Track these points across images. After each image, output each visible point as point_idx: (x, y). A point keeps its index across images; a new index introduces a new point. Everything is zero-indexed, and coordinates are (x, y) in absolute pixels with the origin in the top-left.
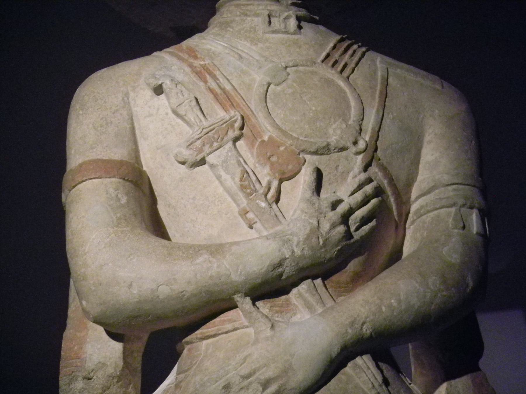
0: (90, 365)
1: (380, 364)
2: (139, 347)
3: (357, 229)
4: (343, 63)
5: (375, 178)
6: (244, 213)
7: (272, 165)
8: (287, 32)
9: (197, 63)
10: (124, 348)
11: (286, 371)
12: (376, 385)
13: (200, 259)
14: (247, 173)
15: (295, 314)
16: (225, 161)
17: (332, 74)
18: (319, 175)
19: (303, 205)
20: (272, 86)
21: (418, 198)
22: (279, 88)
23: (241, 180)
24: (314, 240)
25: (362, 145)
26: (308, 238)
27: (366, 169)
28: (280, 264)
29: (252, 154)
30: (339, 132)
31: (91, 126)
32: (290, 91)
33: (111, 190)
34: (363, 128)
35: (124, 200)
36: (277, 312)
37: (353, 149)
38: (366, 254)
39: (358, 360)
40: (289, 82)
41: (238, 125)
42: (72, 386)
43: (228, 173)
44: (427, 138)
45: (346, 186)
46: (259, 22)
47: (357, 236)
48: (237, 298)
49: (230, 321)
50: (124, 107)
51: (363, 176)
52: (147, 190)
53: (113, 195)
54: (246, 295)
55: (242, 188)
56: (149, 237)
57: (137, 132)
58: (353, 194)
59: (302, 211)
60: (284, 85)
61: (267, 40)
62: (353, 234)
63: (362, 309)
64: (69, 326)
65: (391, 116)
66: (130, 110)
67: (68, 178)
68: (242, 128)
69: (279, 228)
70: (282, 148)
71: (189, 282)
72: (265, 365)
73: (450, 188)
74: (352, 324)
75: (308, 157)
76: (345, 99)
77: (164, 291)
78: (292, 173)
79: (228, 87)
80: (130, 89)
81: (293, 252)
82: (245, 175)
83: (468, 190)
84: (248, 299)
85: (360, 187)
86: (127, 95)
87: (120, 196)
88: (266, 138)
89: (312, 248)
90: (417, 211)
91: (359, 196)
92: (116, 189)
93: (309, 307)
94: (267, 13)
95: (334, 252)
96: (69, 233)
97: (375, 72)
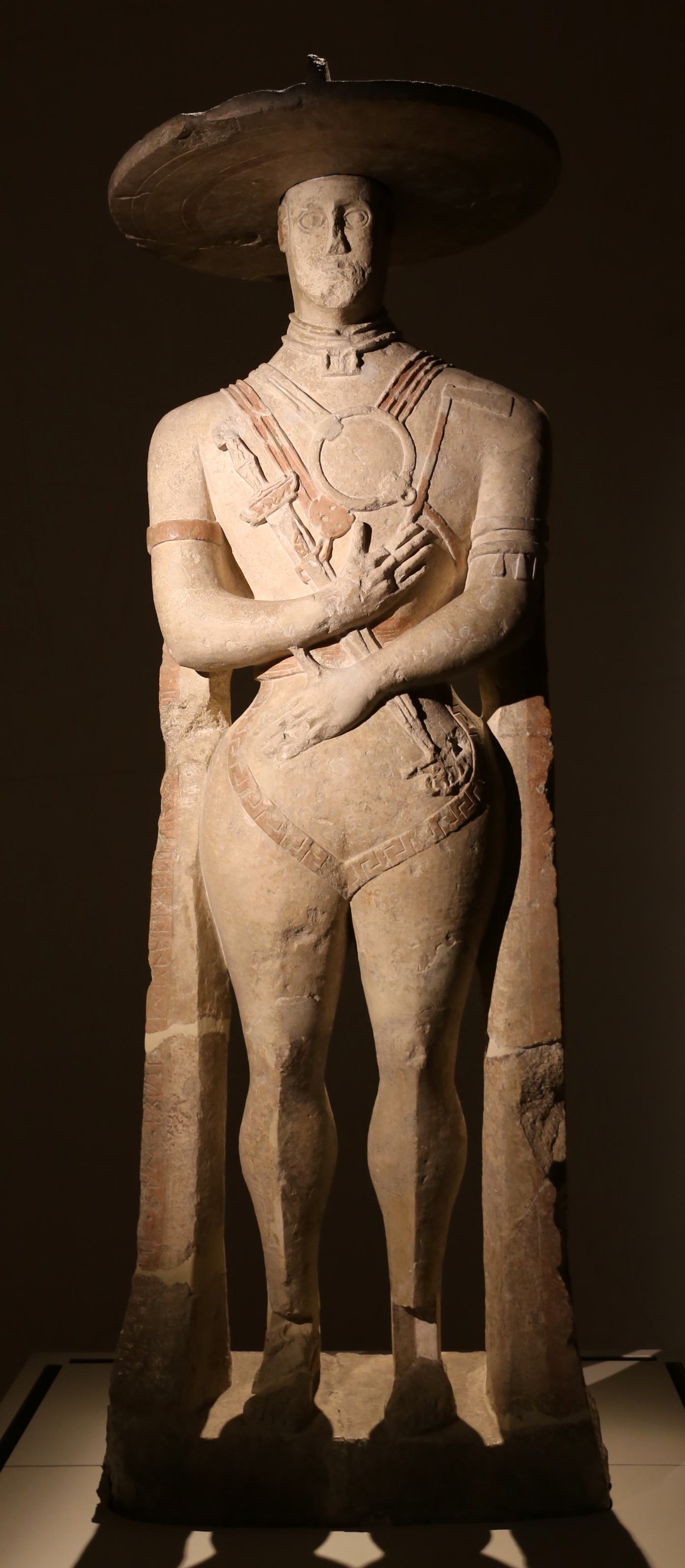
0: (183, 696)
1: (421, 700)
3: (403, 580)
4: (401, 404)
5: (426, 526)
6: (300, 571)
7: (324, 524)
8: (346, 374)
9: (259, 414)
10: (210, 683)
11: (327, 713)
12: (410, 720)
13: (259, 619)
14: (301, 534)
15: (344, 660)
16: (282, 522)
17: (387, 421)
18: (367, 530)
19: (349, 565)
20: (326, 442)
21: (476, 536)
22: (333, 444)
23: (295, 542)
24: (356, 599)
25: (411, 496)
26: (350, 597)
27: (415, 519)
29: (306, 514)
30: (388, 487)
31: (166, 483)
32: (343, 446)
33: (186, 552)
34: (414, 477)
35: (197, 560)
36: (328, 659)
37: (402, 502)
39: (397, 699)
40: (342, 436)
41: (293, 486)
42: (170, 713)
43: (285, 534)
44: (485, 477)
46: (321, 360)
47: (402, 586)
48: (292, 650)
49: (290, 666)
50: (194, 462)
51: (412, 527)
52: (220, 540)
53: (188, 556)
54: (299, 647)
55: (297, 548)
56: (219, 595)
57: (208, 485)
58: (399, 547)
59: (347, 571)
60: (337, 440)
61: (326, 384)
63: (396, 659)
64: (164, 661)
65: (445, 460)
66: (201, 464)
67: (150, 534)
68: (297, 489)
69: (329, 585)
70: (333, 508)
71: (250, 639)
72: (312, 707)
73: (499, 532)
74: (386, 672)
75: (356, 514)
76: (398, 449)
77: (231, 646)
78: (342, 532)
79: (286, 445)
80: (199, 441)
81: (336, 611)
82: (299, 537)
83: (514, 535)
84: (301, 650)
85: (408, 539)
86: (197, 449)
87: (194, 556)
88: (319, 498)
89: (354, 607)
90: (476, 549)
92: (190, 550)
93: (356, 654)
94: (325, 353)
95: (377, 605)
96: (154, 587)
97: (436, 408)
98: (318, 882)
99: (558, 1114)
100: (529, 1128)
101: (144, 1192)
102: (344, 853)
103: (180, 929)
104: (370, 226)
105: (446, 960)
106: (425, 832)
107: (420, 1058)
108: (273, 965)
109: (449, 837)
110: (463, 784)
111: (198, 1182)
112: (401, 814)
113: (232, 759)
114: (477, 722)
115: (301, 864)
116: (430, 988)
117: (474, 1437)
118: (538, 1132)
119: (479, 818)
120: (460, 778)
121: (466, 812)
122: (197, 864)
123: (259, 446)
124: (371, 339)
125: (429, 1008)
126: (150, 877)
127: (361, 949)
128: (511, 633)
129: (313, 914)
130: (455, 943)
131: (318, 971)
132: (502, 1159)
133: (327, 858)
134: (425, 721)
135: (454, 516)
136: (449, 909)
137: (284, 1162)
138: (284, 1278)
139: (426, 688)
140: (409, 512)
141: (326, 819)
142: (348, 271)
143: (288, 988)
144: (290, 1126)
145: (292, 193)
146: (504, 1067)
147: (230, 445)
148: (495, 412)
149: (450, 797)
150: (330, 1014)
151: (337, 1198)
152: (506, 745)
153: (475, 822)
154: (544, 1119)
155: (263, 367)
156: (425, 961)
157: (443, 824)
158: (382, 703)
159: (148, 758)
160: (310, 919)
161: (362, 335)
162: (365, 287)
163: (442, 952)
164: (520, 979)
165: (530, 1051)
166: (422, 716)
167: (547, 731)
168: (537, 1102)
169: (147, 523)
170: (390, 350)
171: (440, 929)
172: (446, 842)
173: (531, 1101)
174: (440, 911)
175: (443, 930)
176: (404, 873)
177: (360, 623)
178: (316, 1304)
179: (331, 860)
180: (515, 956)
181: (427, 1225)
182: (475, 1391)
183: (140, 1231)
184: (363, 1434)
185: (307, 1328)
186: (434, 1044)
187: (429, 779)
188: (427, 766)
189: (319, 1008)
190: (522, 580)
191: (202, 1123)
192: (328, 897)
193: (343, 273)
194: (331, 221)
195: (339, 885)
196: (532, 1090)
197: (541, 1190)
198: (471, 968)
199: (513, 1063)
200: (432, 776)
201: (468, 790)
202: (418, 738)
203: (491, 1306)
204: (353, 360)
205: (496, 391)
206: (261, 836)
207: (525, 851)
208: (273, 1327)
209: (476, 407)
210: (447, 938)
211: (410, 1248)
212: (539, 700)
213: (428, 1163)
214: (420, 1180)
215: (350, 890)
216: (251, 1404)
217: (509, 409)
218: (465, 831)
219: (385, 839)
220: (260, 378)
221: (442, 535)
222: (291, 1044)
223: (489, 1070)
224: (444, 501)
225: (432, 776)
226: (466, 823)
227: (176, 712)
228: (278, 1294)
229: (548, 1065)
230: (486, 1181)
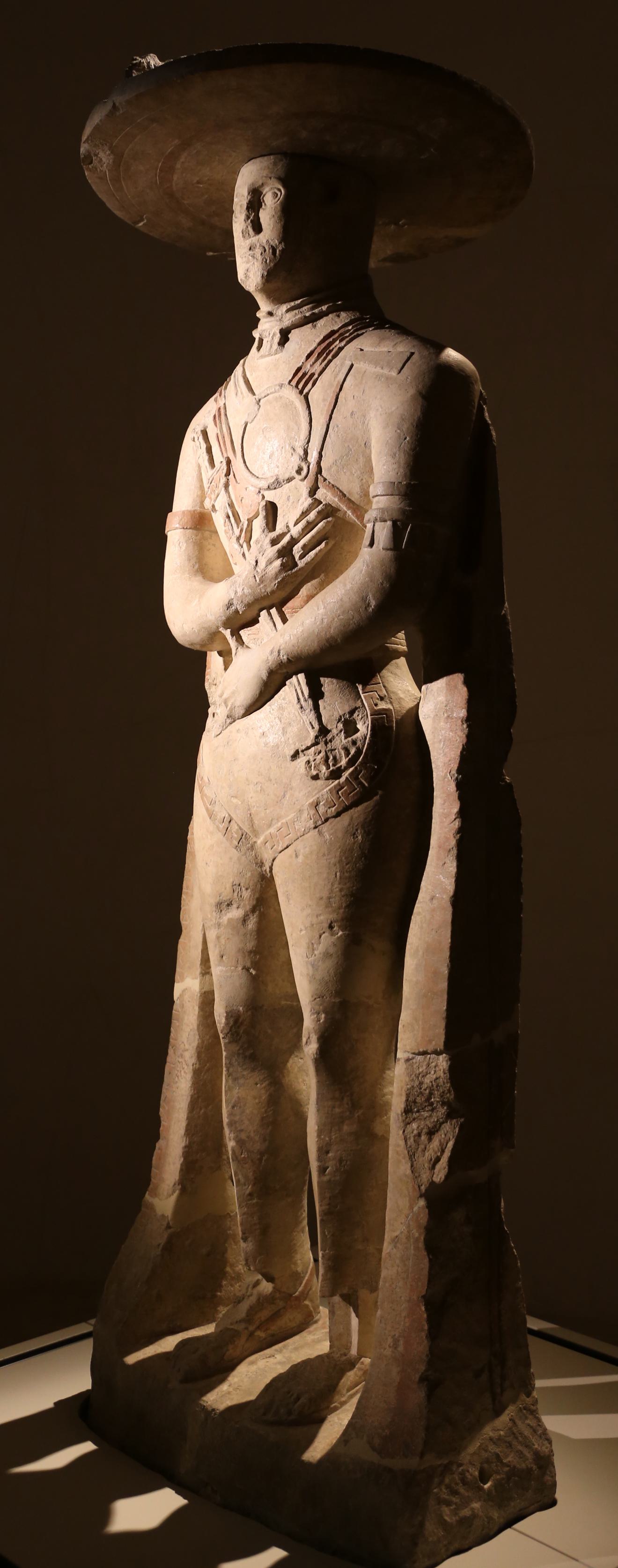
1: (322, 679)
3: (302, 557)
24: (252, 580)
28: (230, 605)
34: (309, 451)
37: (298, 477)
38: (322, 576)
47: (301, 564)
62: (299, 562)
74: (272, 652)
81: (236, 592)
85: (304, 514)
89: (251, 587)
98: (239, 859)
100: (412, 1139)
102: (256, 834)
104: (281, 203)
105: (332, 950)
109: (328, 823)
110: (346, 768)
111: (188, 1125)
112: (287, 796)
115: (224, 840)
116: (318, 977)
118: (422, 1146)
119: (365, 804)
120: (343, 762)
121: (347, 798)
125: (321, 996)
129: (237, 889)
130: (340, 933)
131: (250, 945)
134: (320, 702)
136: (329, 898)
140: (304, 487)
141: (236, 797)
142: (258, 251)
143: (224, 958)
144: (236, 1091)
148: (386, 371)
149: (331, 781)
153: (360, 808)
154: (431, 1133)
157: (322, 809)
160: (236, 894)
161: (297, 311)
162: (275, 265)
164: (415, 979)
165: (419, 1058)
167: (463, 713)
168: (426, 1114)
171: (322, 918)
172: (325, 828)
173: (418, 1111)
174: (321, 898)
175: (325, 918)
176: (291, 856)
177: (266, 603)
179: (246, 838)
187: (308, 762)
188: (308, 748)
190: (387, 549)
192: (249, 874)
193: (253, 257)
195: (257, 864)
196: (418, 1100)
197: (415, 1209)
200: (312, 759)
201: (351, 774)
210: (331, 927)
212: (458, 679)
213: (330, 1155)
215: (267, 867)
217: (400, 365)
218: (345, 818)
219: (278, 821)
221: (343, 507)
222: (226, 1012)
224: (338, 472)
225: (312, 759)
226: (346, 809)
229: (434, 1077)
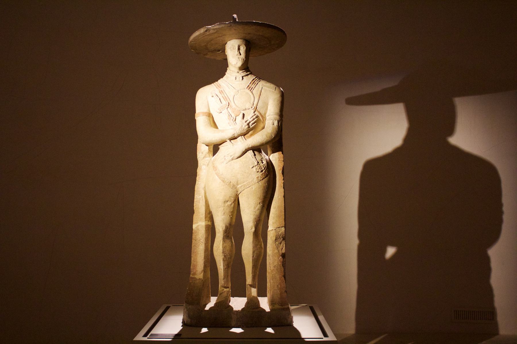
2: (212, 147)
17: (248, 91)
18: (244, 115)
25: (253, 108)
44: (269, 104)
45: (250, 116)
47: (251, 127)
67: (196, 115)
77: (214, 139)
91: (252, 119)
99: (283, 242)
101: (192, 259)
102: (238, 184)
103: (201, 202)
106: (255, 180)
107: (253, 229)
108: (222, 209)
113: (213, 164)
114: (267, 157)
117: (264, 310)
120: (263, 169)
122: (205, 187)
123: (220, 96)
124: (245, 74)
126: (194, 190)
127: (241, 206)
128: (274, 137)
131: (232, 210)
132: (271, 252)
133: (234, 186)
135: (263, 112)
137: (223, 252)
138: (223, 278)
139: (256, 149)
140: (253, 111)
142: (240, 59)
145: (228, 42)
146: (272, 232)
147: (214, 96)
150: (234, 220)
151: (235, 262)
152: (273, 162)
155: (221, 79)
156: (255, 208)
157: (259, 178)
158: (246, 152)
159: (194, 164)
163: (259, 206)
166: (255, 155)
167: (282, 159)
169: (195, 112)
170: (249, 76)
175: (259, 201)
178: (230, 285)
180: (275, 208)
181: (255, 267)
182: (264, 304)
183: (192, 267)
184: (240, 309)
185: (228, 289)
186: (257, 227)
189: (231, 218)
191: (205, 244)
194: (237, 49)
198: (265, 210)
199: (274, 231)
202: (254, 159)
203: (268, 285)
204: (241, 78)
205: (272, 86)
206: (219, 181)
207: (277, 185)
208: (220, 289)
209: (268, 89)
211: (251, 272)
212: (281, 152)
214: (253, 256)
216: (216, 304)
220: (220, 81)
221: (260, 116)
223: (269, 233)
227: (201, 154)
228: (221, 281)
230: (267, 257)
